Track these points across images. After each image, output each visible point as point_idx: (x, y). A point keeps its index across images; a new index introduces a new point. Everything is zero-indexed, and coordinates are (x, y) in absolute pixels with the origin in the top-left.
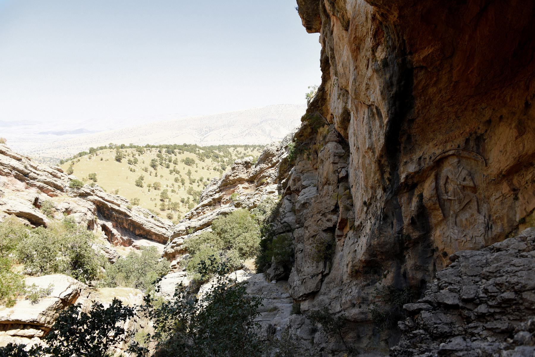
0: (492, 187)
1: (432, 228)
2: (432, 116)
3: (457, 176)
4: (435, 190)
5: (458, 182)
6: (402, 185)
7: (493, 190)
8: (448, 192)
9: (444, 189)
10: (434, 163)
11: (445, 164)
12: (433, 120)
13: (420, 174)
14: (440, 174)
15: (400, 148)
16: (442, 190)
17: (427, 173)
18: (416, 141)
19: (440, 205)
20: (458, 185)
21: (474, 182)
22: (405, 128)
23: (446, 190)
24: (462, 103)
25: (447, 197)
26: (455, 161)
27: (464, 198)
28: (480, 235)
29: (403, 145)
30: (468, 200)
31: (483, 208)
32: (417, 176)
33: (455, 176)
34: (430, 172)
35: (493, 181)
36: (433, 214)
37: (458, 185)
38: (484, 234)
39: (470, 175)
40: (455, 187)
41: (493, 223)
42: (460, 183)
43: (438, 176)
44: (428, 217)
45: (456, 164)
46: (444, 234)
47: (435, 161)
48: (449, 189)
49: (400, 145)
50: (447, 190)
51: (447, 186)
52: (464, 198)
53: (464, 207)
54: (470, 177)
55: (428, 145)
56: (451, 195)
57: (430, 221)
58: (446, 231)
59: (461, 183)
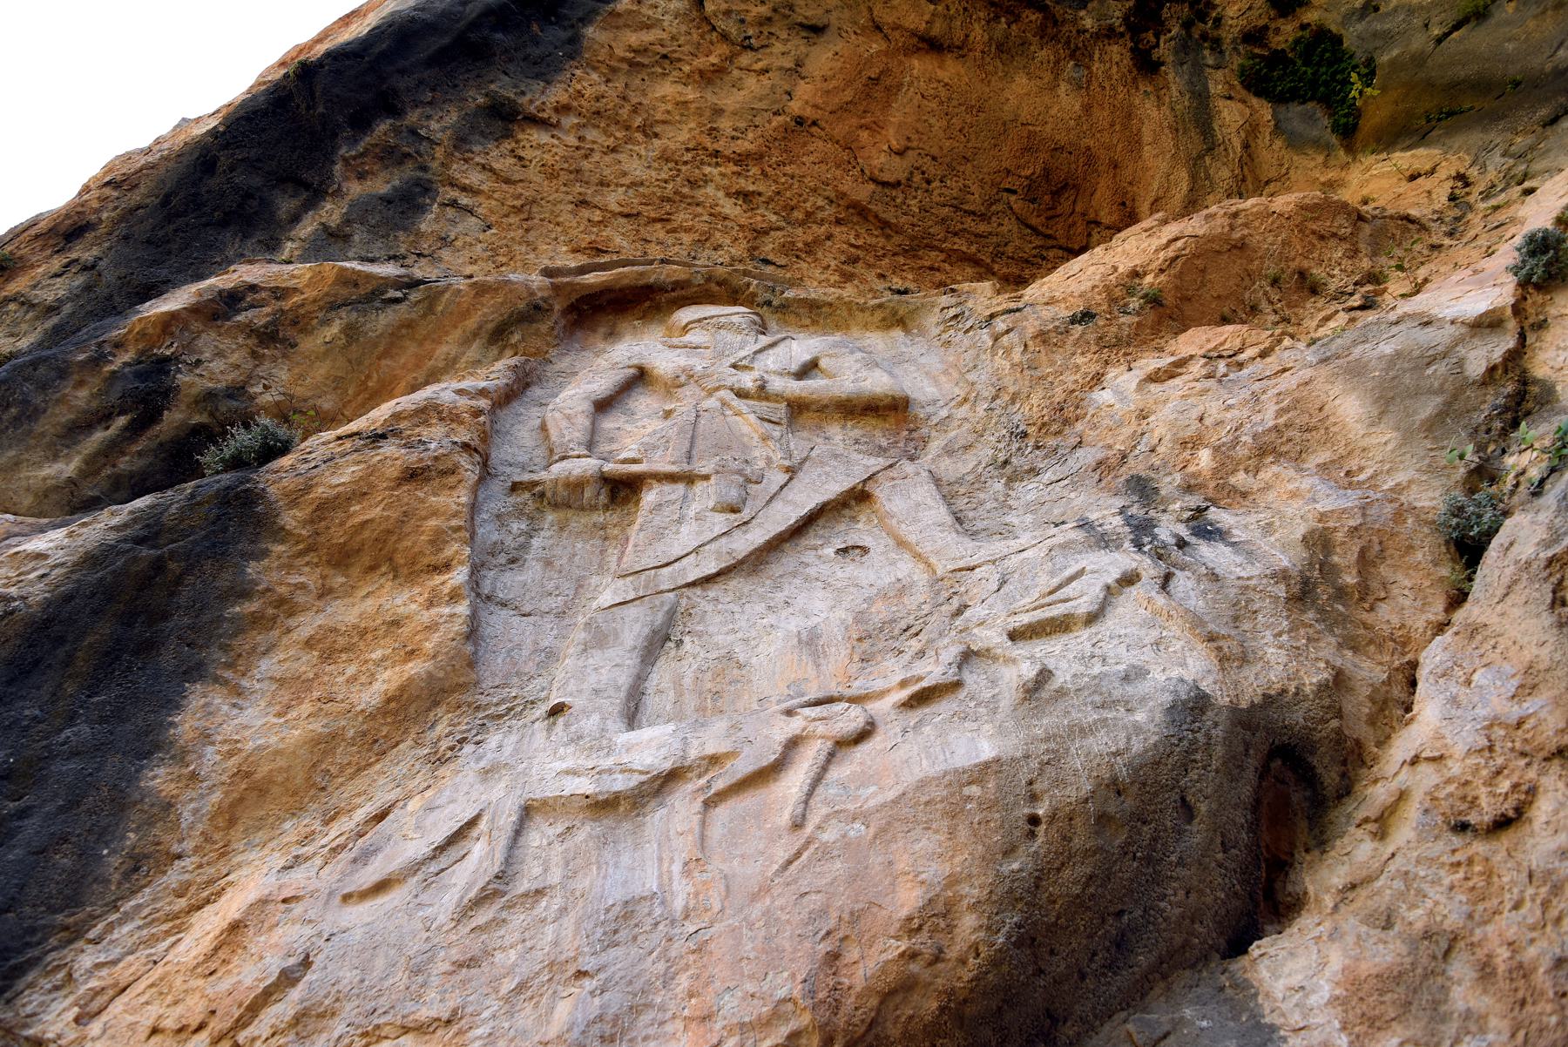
1: (140, 867)
2: (626, 181)
6: (98, 361)
12: (613, 199)
13: (384, 320)
15: (295, 219)
17: (443, 350)
18: (445, 241)
22: (434, 125)
24: (798, 215)
29: (331, 212)
32: (335, 329)
34: (473, 352)
36: (307, 625)
44: (195, 672)
49: (312, 203)
57: (185, 725)
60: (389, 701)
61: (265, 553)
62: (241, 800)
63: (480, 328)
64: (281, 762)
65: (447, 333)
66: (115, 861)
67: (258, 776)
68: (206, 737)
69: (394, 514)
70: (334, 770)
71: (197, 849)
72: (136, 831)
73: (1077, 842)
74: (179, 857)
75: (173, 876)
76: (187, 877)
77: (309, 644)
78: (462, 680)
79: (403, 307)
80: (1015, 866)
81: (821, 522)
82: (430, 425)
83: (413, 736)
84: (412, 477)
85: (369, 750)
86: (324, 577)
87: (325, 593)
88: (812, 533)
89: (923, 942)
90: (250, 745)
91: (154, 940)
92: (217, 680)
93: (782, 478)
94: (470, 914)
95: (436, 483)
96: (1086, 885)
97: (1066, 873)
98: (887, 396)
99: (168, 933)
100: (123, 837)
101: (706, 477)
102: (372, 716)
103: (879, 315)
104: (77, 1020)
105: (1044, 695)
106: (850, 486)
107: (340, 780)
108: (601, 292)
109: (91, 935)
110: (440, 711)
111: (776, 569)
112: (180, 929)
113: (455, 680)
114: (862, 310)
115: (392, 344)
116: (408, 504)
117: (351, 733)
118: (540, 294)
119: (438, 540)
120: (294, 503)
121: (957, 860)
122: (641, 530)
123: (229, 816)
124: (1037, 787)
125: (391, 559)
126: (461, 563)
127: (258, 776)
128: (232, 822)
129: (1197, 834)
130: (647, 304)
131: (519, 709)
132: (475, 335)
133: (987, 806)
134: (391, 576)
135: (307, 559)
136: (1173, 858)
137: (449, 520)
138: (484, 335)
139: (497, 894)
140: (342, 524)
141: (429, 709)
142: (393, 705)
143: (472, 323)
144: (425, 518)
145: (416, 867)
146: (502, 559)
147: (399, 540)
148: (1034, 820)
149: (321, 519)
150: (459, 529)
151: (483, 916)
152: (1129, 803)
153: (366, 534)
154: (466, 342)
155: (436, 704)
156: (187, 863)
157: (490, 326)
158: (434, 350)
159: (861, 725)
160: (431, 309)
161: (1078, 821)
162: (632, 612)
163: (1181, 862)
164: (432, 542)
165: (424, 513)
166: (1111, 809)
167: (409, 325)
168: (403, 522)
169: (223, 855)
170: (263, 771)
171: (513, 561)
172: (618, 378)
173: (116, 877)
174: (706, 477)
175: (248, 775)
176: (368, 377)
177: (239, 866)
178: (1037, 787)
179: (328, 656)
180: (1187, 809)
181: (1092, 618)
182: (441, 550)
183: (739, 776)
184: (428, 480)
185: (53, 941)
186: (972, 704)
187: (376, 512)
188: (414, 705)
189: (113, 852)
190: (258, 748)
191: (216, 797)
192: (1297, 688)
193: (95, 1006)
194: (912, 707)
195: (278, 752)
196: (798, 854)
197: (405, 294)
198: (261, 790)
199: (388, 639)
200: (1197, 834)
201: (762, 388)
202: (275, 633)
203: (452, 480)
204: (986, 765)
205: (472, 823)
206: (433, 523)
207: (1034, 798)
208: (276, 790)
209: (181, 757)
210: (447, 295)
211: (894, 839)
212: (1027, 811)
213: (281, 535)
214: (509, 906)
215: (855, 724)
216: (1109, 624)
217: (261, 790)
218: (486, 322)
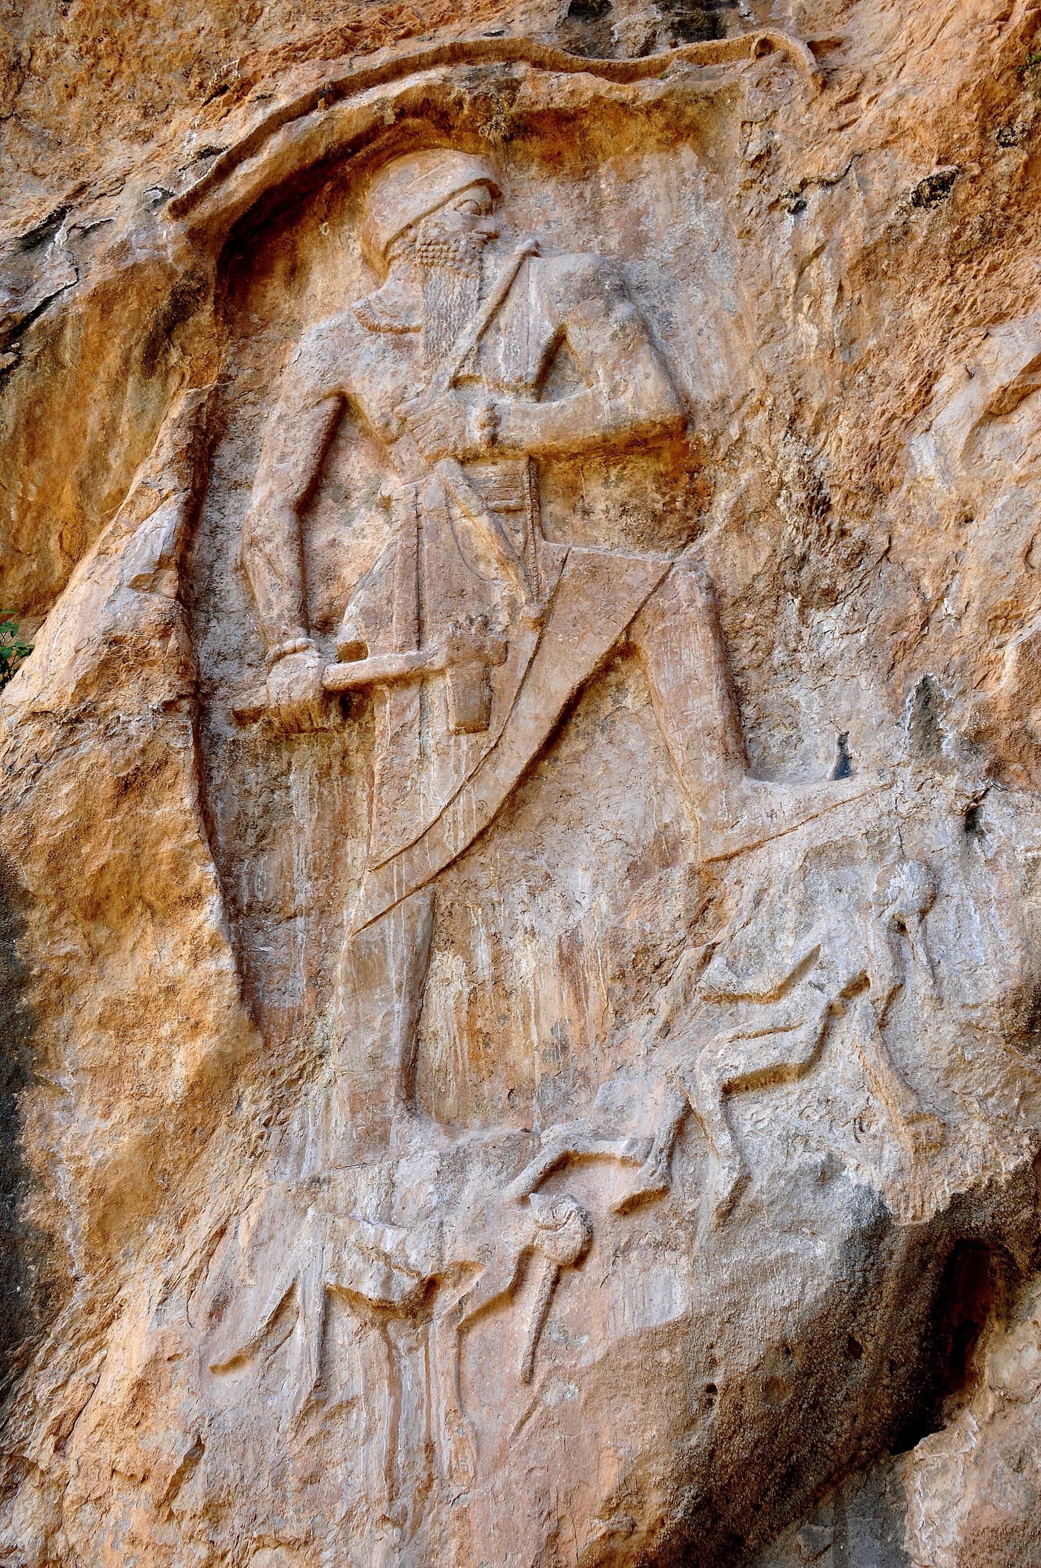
0: (918, 309)
3: (465, 342)
4: (168, 583)
5: (477, 414)
7: (926, 341)
8: (326, 626)
9: (287, 564)
10: (194, 235)
11: (318, 280)
14: (252, 426)
16: (263, 581)
19: (202, 798)
20: (467, 459)
21: (666, 368)
23: (305, 589)
25: (310, 660)
26: (443, 188)
27: (541, 623)
28: (802, 1037)
30: (596, 648)
31: (798, 694)
33: (435, 353)
35: (922, 219)
37: (467, 459)
38: (879, 987)
39: (623, 291)
40: (431, 496)
41: (996, 770)
42: (494, 420)
43: (227, 452)
45: (452, 219)
46: (217, 1310)
47: (204, 210)
48: (349, 574)
50: (321, 597)
51: (320, 538)
52: (541, 623)
53: (530, 773)
54: (622, 310)
55: (147, 137)
56: (374, 618)
58: (257, 1244)
59: (511, 431)
60: (192, 1088)
61: (24, 925)
62: (105, 1216)
63: (126, 361)
64: (124, 1173)
65: (88, 388)
66: (30, 1294)
67: (110, 1191)
68: (53, 1159)
69: (125, 849)
70: (170, 1168)
71: (87, 1268)
72: (34, 1262)
73: (747, 1411)
74: (76, 1279)
75: (78, 1300)
76: (89, 1295)
77: (102, 1023)
78: (250, 1048)
79: (21, 374)
80: (694, 1442)
81: (581, 709)
82: (121, 686)
83: (225, 1120)
84: (126, 786)
85: (192, 1140)
86: (86, 936)
87: (94, 955)
88: (572, 731)
89: (619, 1520)
90: (91, 1162)
91: (85, 1359)
92: (38, 1081)
93: (532, 638)
94: (304, 1423)
95: (153, 785)
96: (756, 1446)
97: (737, 1440)
98: (654, 424)
99: (94, 1351)
100: (27, 1271)
101: (441, 672)
102: (183, 1107)
103: (659, 119)
104: (57, 1448)
105: (738, 1213)
106: (612, 642)
107: (178, 1176)
108: (260, 200)
109: (38, 1361)
110: (240, 1084)
111: (536, 811)
112: (100, 1346)
113: (244, 1051)
114: (633, 116)
115: (31, 436)
116: (135, 831)
117: (171, 1128)
118: (181, 269)
119: (179, 866)
120: (25, 857)
121: (647, 1436)
122: (382, 784)
123: (102, 1230)
124: (718, 1352)
125: (141, 897)
126: (210, 891)
127: (110, 1191)
128: (105, 1238)
129: (863, 1369)
130: (328, 187)
131: (309, 1068)
132: (125, 370)
133: (676, 1371)
134: (149, 915)
135: (63, 920)
136: (839, 1398)
137: (181, 837)
138: (136, 367)
139: (321, 1403)
140: (81, 873)
141: (230, 1086)
142: (197, 1091)
143: (113, 359)
144: (158, 843)
145: (255, 1347)
146: (251, 841)
147: (141, 878)
148: (711, 1389)
149: (59, 870)
150: (192, 846)
151: (312, 1428)
152: (797, 1362)
153: (107, 881)
154: (116, 387)
155: (234, 1078)
156: (87, 1281)
157: (137, 353)
158: (83, 421)
159: (579, 1247)
160: (58, 364)
161: (749, 1390)
162: (388, 924)
163: (847, 1398)
164: (174, 871)
165: (154, 837)
166: (779, 1373)
167: (40, 399)
168: (137, 856)
169: (110, 1268)
170: (112, 1184)
171: (261, 837)
172: (319, 424)
173: (36, 1308)
174: (441, 672)
175: (101, 1192)
176: (25, 491)
177: (125, 1279)
178: (718, 1352)
179: (123, 1034)
180: (854, 1350)
181: (806, 1069)
182: (184, 878)
183: (484, 1301)
184: (144, 785)
185: (12, 1372)
186: (674, 1223)
187: (106, 854)
188: (216, 1087)
189: (25, 1287)
190: (100, 1164)
191: (84, 1220)
192: (990, 1180)
193: (63, 1431)
194: (625, 1213)
195: (117, 1165)
196: (529, 1415)
197: (17, 351)
198: (117, 1202)
199: (170, 1010)
200: (863, 1369)
201: (493, 439)
202: (68, 1014)
203: (168, 774)
204: (676, 1325)
205: (290, 1294)
206: (167, 847)
207: (713, 1363)
208: (129, 1199)
209: (40, 1183)
210: (68, 334)
211: (600, 1407)
212: (706, 1380)
213: (27, 900)
214: (331, 1416)
215: (573, 1244)
216: (823, 1074)
217: (117, 1202)
218: (130, 349)
